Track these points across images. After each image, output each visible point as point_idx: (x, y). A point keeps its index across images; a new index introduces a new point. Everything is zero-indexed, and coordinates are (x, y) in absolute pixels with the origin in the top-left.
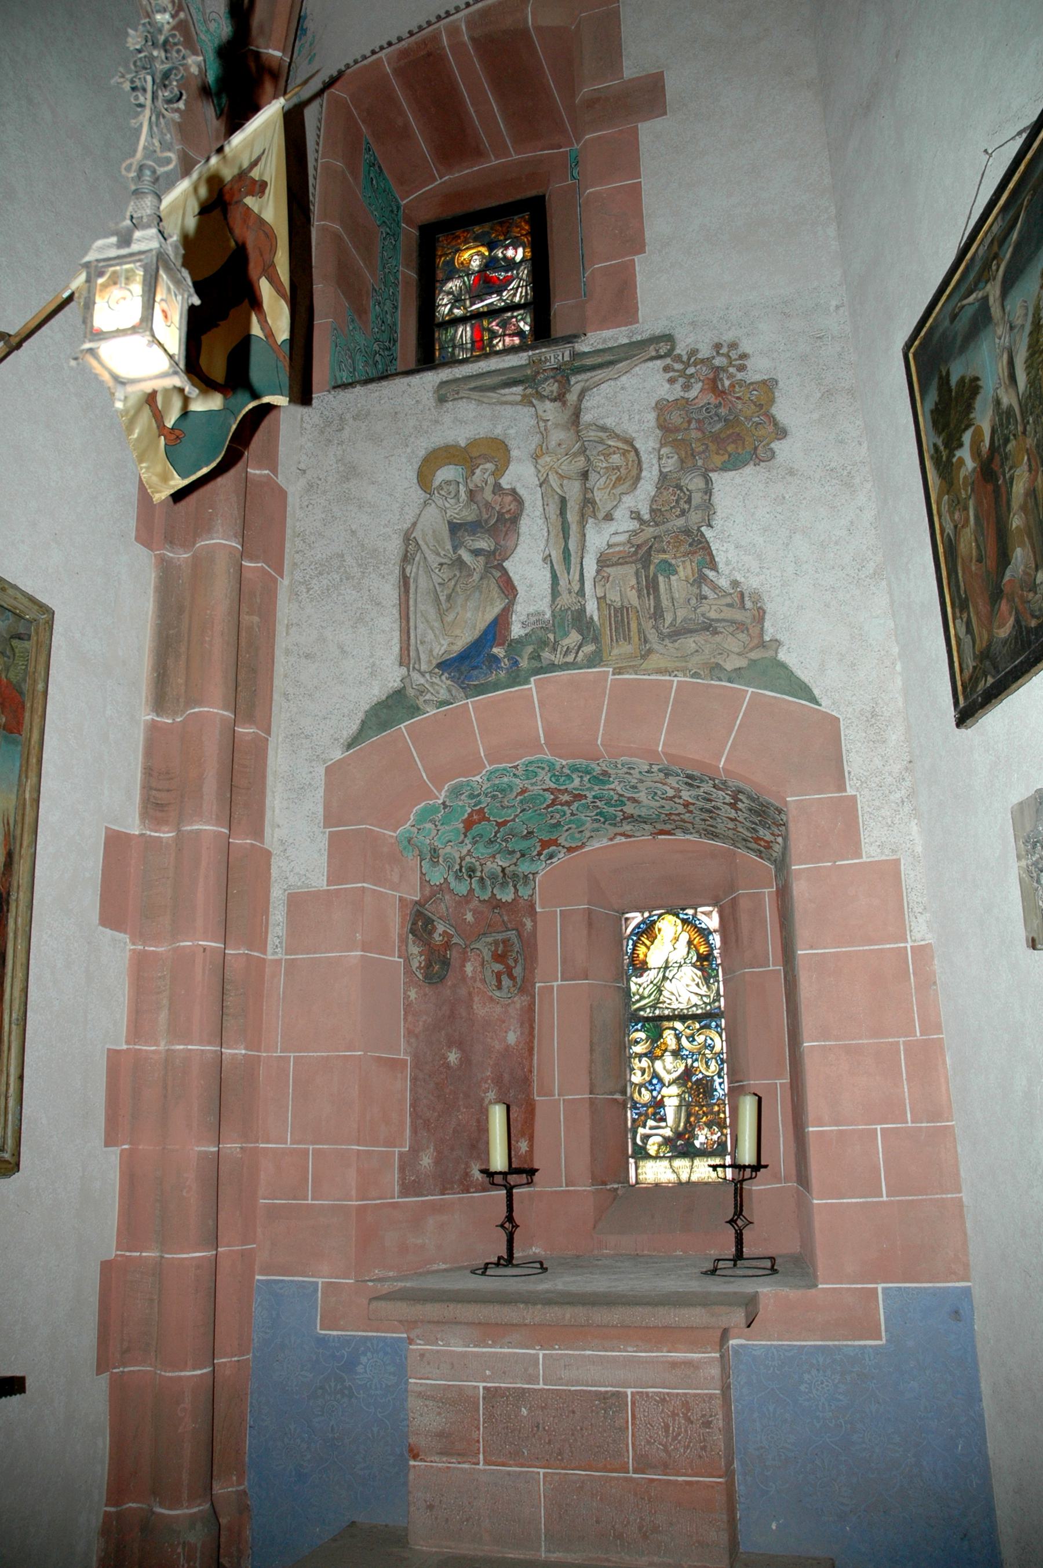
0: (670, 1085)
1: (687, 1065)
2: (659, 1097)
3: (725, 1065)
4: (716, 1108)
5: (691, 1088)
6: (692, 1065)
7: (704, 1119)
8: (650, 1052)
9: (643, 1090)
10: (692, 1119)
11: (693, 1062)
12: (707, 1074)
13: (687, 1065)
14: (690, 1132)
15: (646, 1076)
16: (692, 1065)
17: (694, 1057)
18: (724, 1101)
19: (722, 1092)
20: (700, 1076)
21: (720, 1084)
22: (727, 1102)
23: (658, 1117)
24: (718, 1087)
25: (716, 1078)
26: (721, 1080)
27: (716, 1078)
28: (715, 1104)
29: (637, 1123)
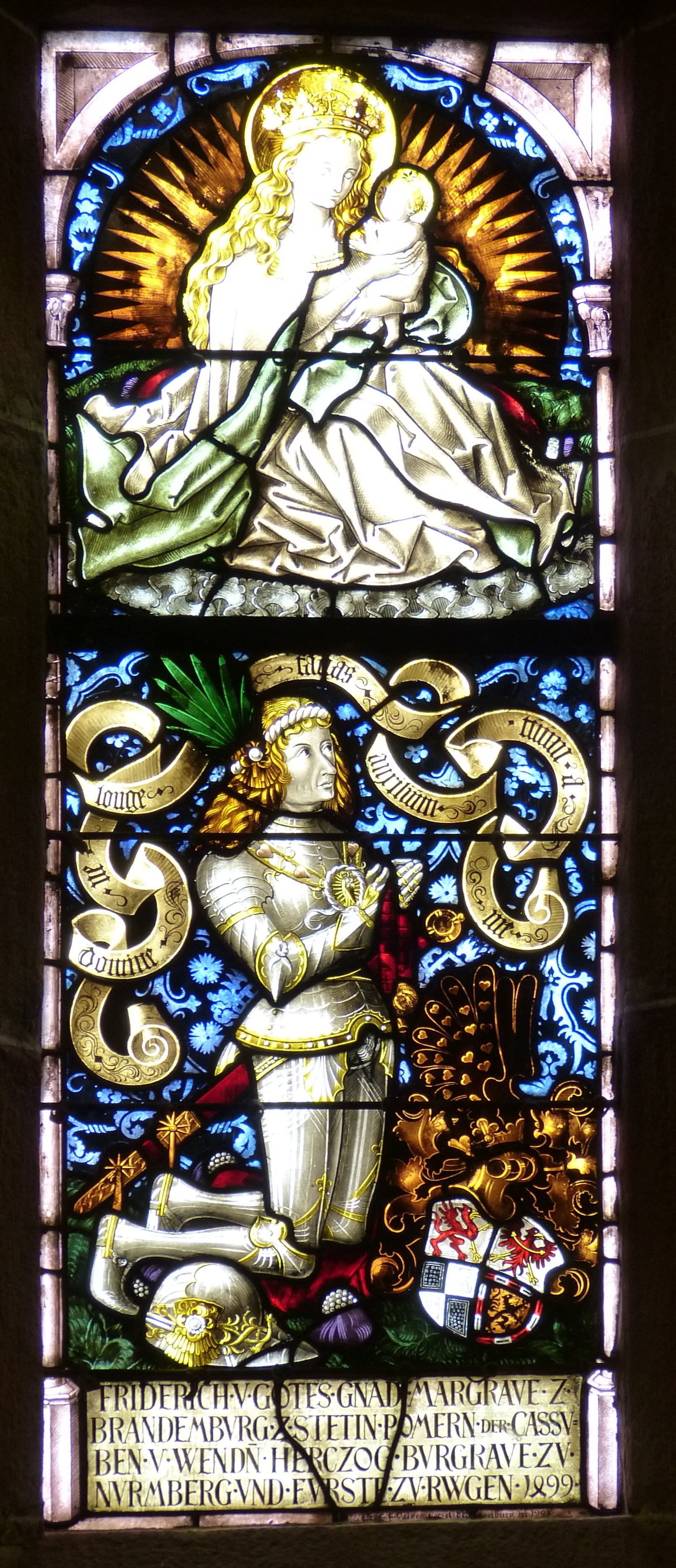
0: (287, 996)
1: (391, 888)
2: (229, 1055)
3: (609, 901)
4: (550, 1126)
5: (415, 1017)
6: (422, 899)
7: (479, 1179)
8: (184, 807)
9: (136, 1014)
10: (411, 1177)
11: (430, 877)
12: (508, 941)
13: (391, 888)
14: (394, 1244)
15: (153, 940)
16: (422, 899)
17: (438, 852)
18: (595, 1084)
19: (581, 1042)
20: (468, 950)
21: (576, 999)
22: (607, 1093)
23: (218, 1160)
24: (561, 1012)
25: (553, 964)
26: (584, 979)
27: (553, 964)
28: (542, 1104)
29: (98, 1192)
